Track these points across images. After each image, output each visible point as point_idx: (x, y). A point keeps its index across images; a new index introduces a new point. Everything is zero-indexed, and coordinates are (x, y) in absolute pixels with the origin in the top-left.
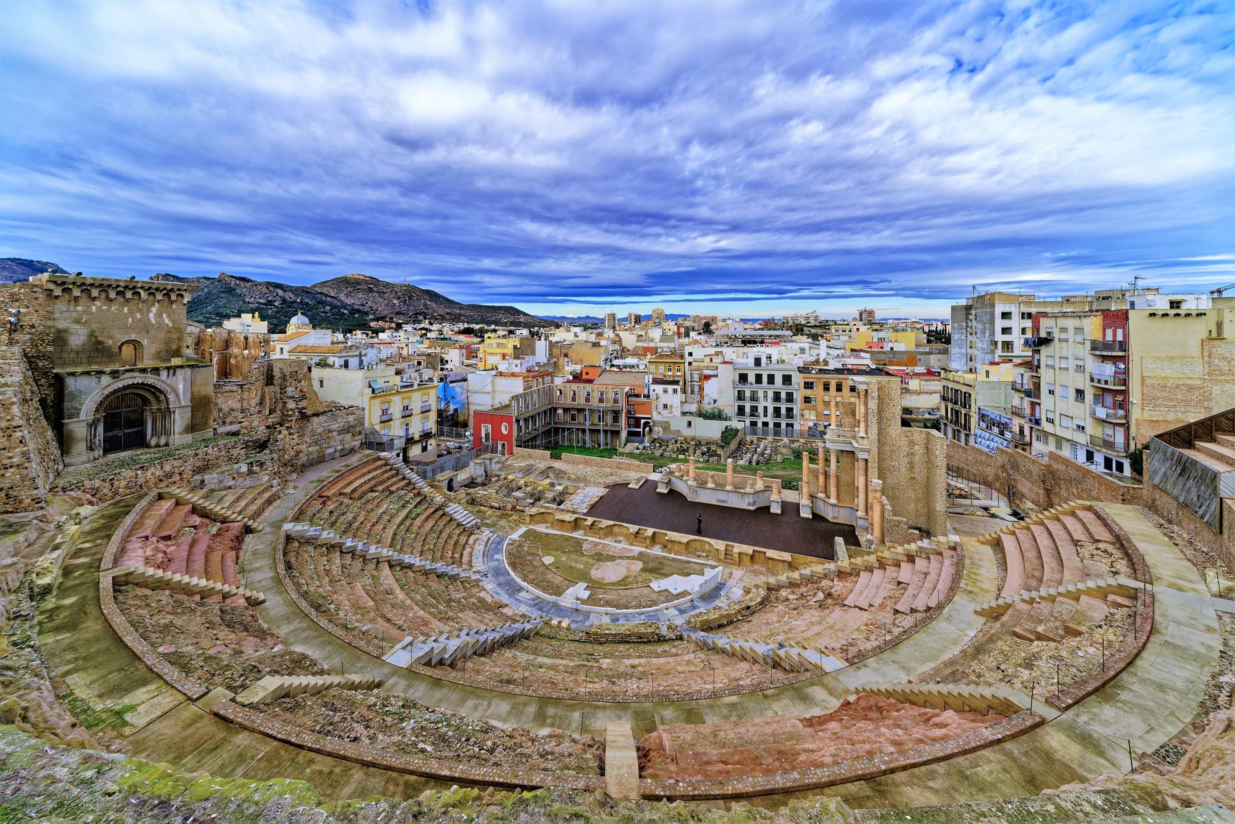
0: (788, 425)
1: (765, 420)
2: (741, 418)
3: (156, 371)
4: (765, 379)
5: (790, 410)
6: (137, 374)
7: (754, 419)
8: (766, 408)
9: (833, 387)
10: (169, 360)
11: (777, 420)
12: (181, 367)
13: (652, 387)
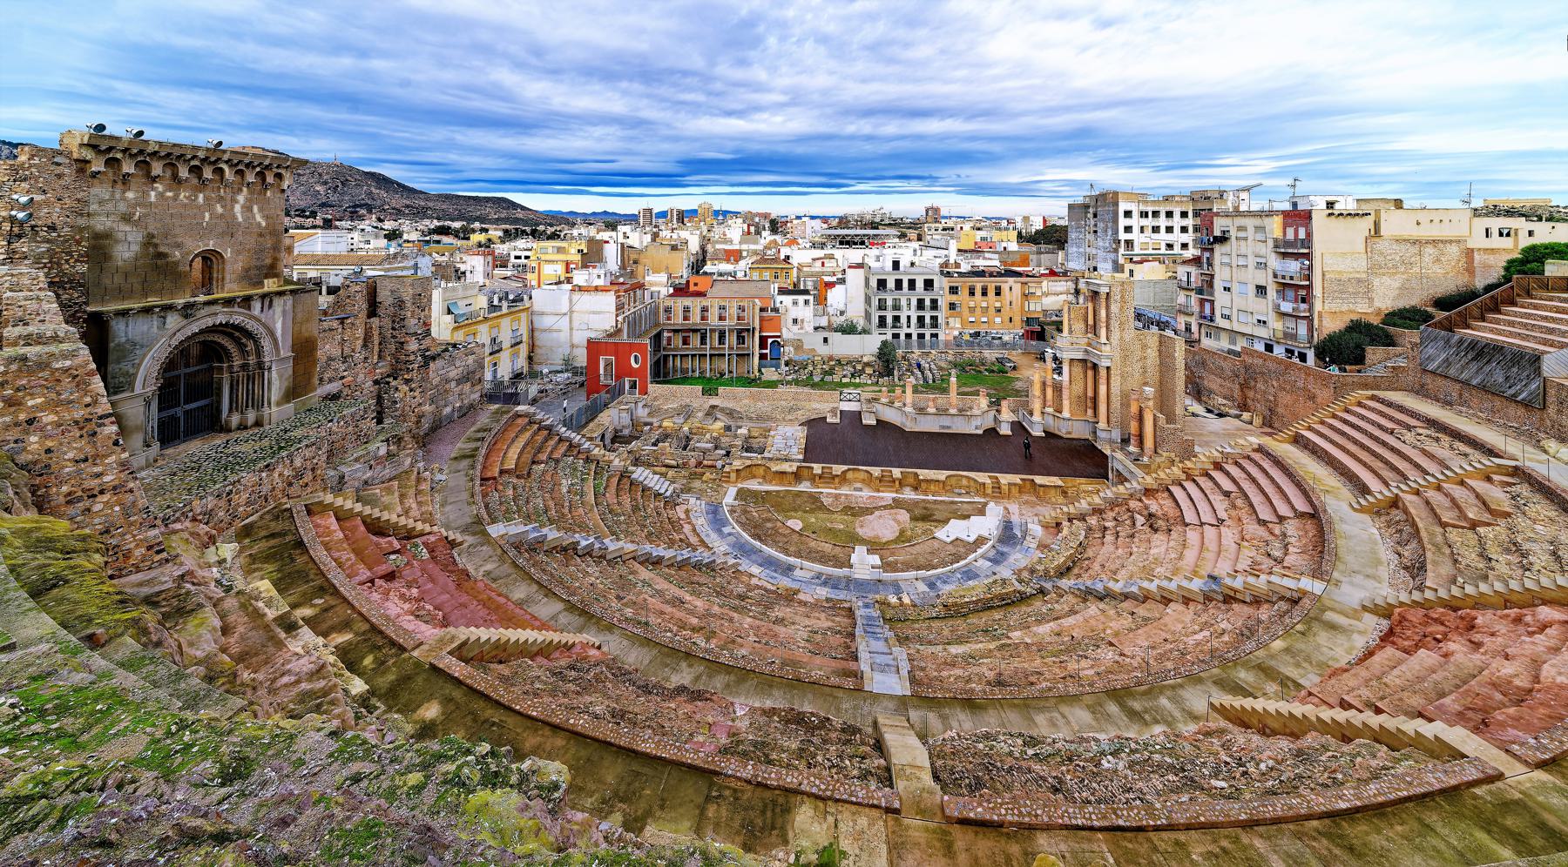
0: (933, 335)
2: (883, 330)
3: (247, 301)
4: (905, 285)
5: (934, 318)
6: (218, 308)
7: (896, 331)
9: (978, 291)
10: (261, 284)
11: (921, 331)
12: (281, 294)
13: (779, 298)
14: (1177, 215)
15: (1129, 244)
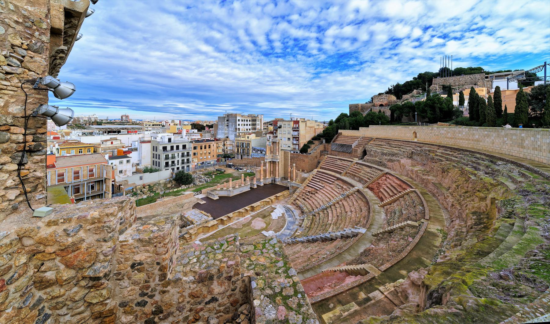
0: (187, 166)
1: (178, 166)
2: (167, 168)
4: (175, 148)
5: (188, 160)
8: (178, 161)
13: (111, 162)
15: (239, 129)
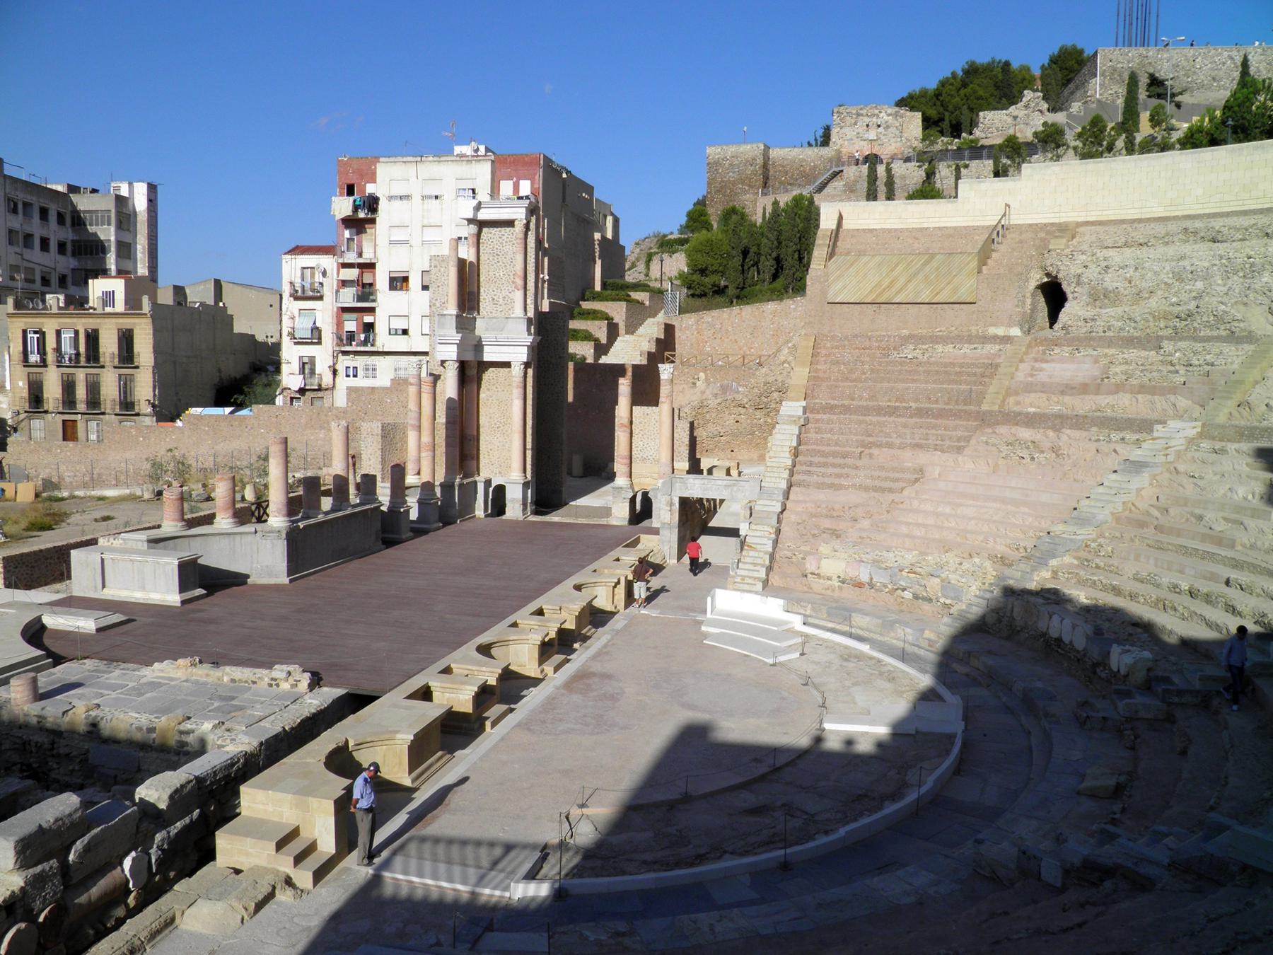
14: (53, 218)
